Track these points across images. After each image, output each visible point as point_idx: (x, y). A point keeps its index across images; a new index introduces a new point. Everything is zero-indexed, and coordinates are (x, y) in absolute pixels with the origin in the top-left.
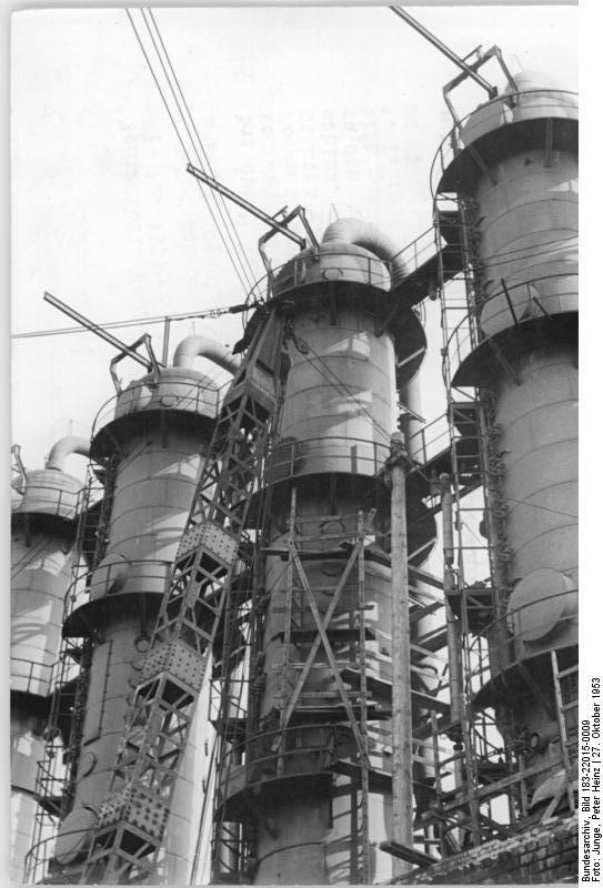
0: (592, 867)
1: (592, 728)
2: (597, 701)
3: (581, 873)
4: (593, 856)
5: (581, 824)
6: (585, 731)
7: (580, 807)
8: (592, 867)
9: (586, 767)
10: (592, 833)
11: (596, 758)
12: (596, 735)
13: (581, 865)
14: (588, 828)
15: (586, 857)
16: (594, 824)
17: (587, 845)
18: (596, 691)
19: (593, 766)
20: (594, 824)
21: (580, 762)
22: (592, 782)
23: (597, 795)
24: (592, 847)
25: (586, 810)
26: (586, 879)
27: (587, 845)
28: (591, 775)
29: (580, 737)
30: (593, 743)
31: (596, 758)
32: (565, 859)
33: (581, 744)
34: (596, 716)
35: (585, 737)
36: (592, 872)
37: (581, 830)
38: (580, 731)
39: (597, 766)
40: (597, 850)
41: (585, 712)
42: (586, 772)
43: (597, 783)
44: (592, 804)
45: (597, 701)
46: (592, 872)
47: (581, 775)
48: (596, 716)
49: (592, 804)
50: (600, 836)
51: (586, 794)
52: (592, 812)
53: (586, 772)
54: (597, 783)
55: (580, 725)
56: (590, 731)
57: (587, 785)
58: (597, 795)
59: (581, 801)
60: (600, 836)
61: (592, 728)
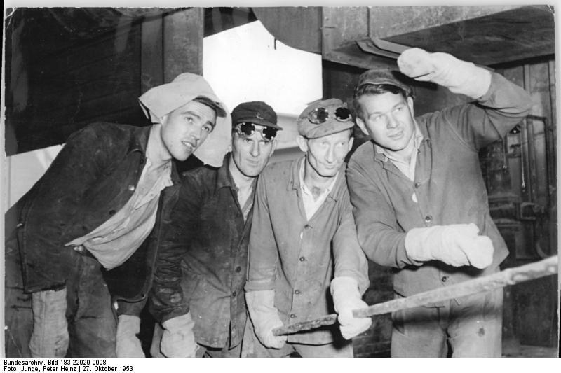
0: (14, 366)
1: (101, 366)
2: (118, 369)
3: (9, 359)
4: (21, 367)
5: (41, 359)
6: (99, 362)
7: (50, 359)
8: (14, 366)
9: (77, 362)
10: (35, 366)
11: (82, 369)
12: (96, 368)
13: (14, 359)
14: (38, 363)
15: (20, 363)
16: (40, 367)
17: (27, 363)
18: (124, 368)
19: (77, 366)
20: (40, 367)
21: (80, 359)
22: (67, 366)
23: (59, 369)
24: (26, 366)
25: (50, 362)
26: (5, 362)
27: (27, 363)
28: (71, 365)
29: (96, 359)
30: (92, 366)
31: (82, 369)
32: (18, 346)
33: (91, 359)
34: (108, 369)
35: (96, 362)
36: (10, 366)
37: (36, 359)
38: (99, 359)
39: (77, 369)
40: (24, 369)
41: (110, 362)
42: (73, 362)
43: (66, 369)
44: (53, 366)
45: (118, 369)
46: (10, 366)
47: (71, 359)
48: (108, 369)
49: (53, 366)
50: (33, 371)
51: (59, 362)
52: (48, 366)
53: (73, 362)
54: (66, 369)
55: (103, 359)
56: (99, 365)
57: (65, 363)
58: (59, 369)
59: (55, 359)
60: (33, 371)
61: (101, 366)
